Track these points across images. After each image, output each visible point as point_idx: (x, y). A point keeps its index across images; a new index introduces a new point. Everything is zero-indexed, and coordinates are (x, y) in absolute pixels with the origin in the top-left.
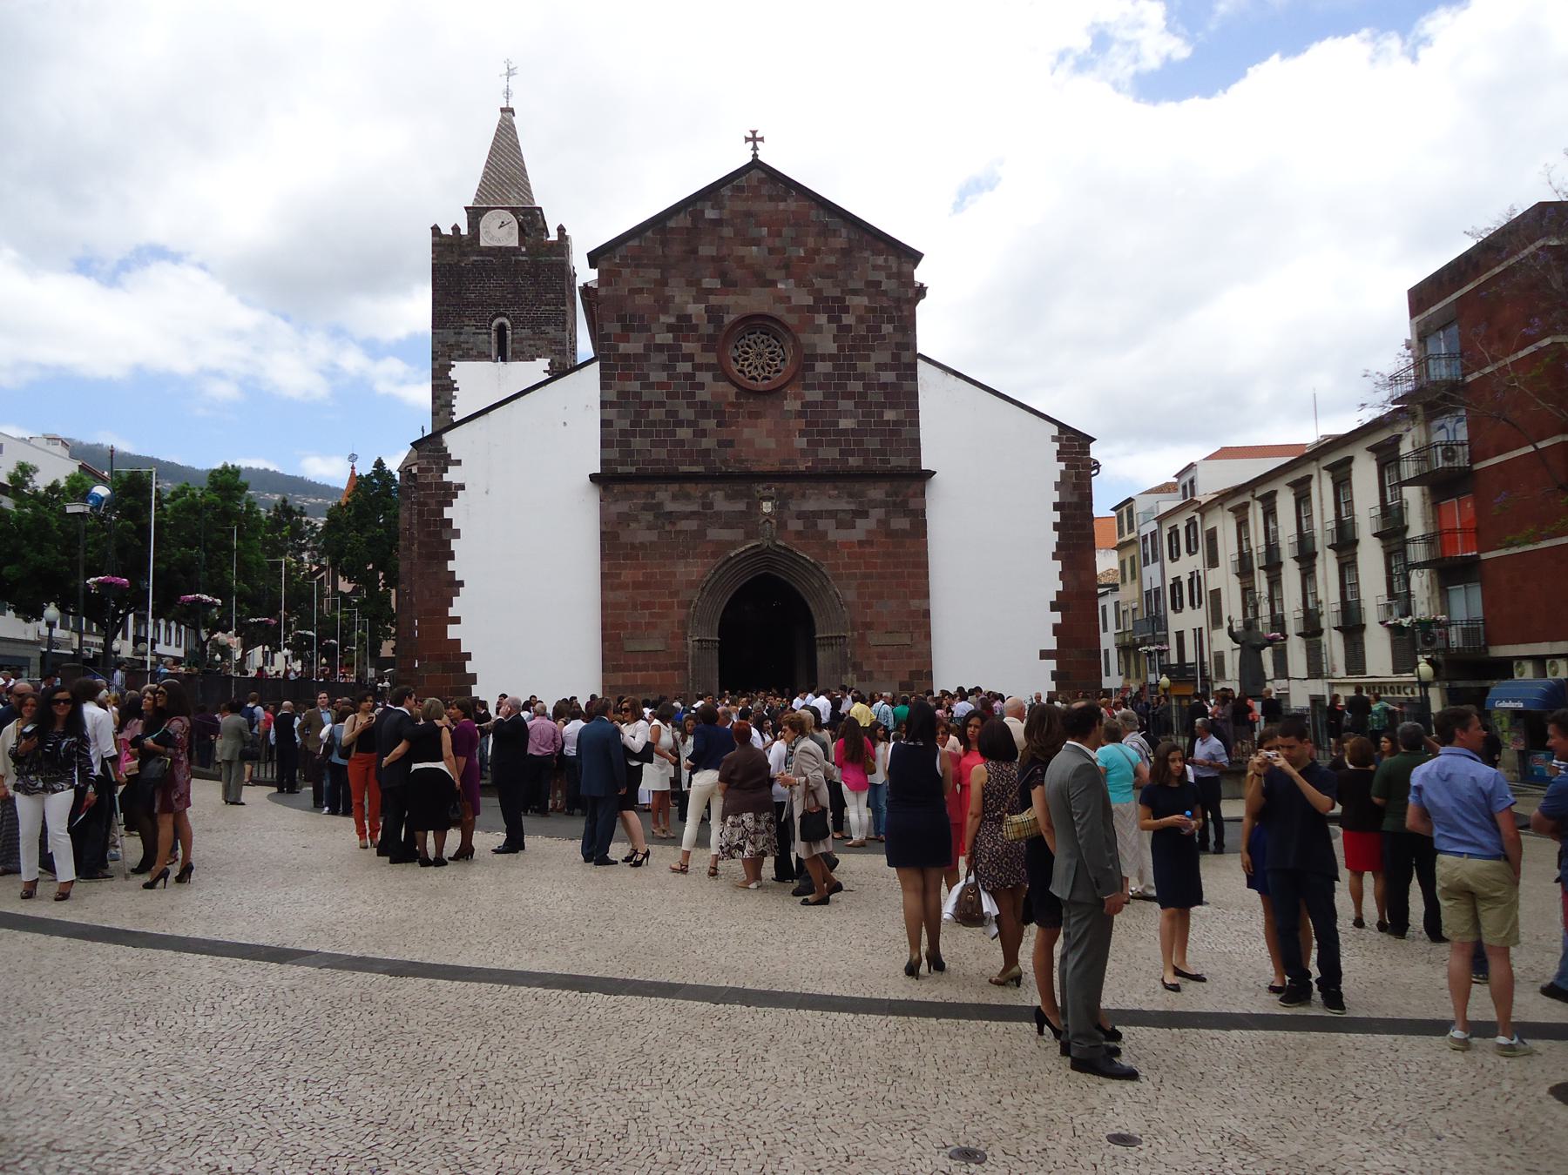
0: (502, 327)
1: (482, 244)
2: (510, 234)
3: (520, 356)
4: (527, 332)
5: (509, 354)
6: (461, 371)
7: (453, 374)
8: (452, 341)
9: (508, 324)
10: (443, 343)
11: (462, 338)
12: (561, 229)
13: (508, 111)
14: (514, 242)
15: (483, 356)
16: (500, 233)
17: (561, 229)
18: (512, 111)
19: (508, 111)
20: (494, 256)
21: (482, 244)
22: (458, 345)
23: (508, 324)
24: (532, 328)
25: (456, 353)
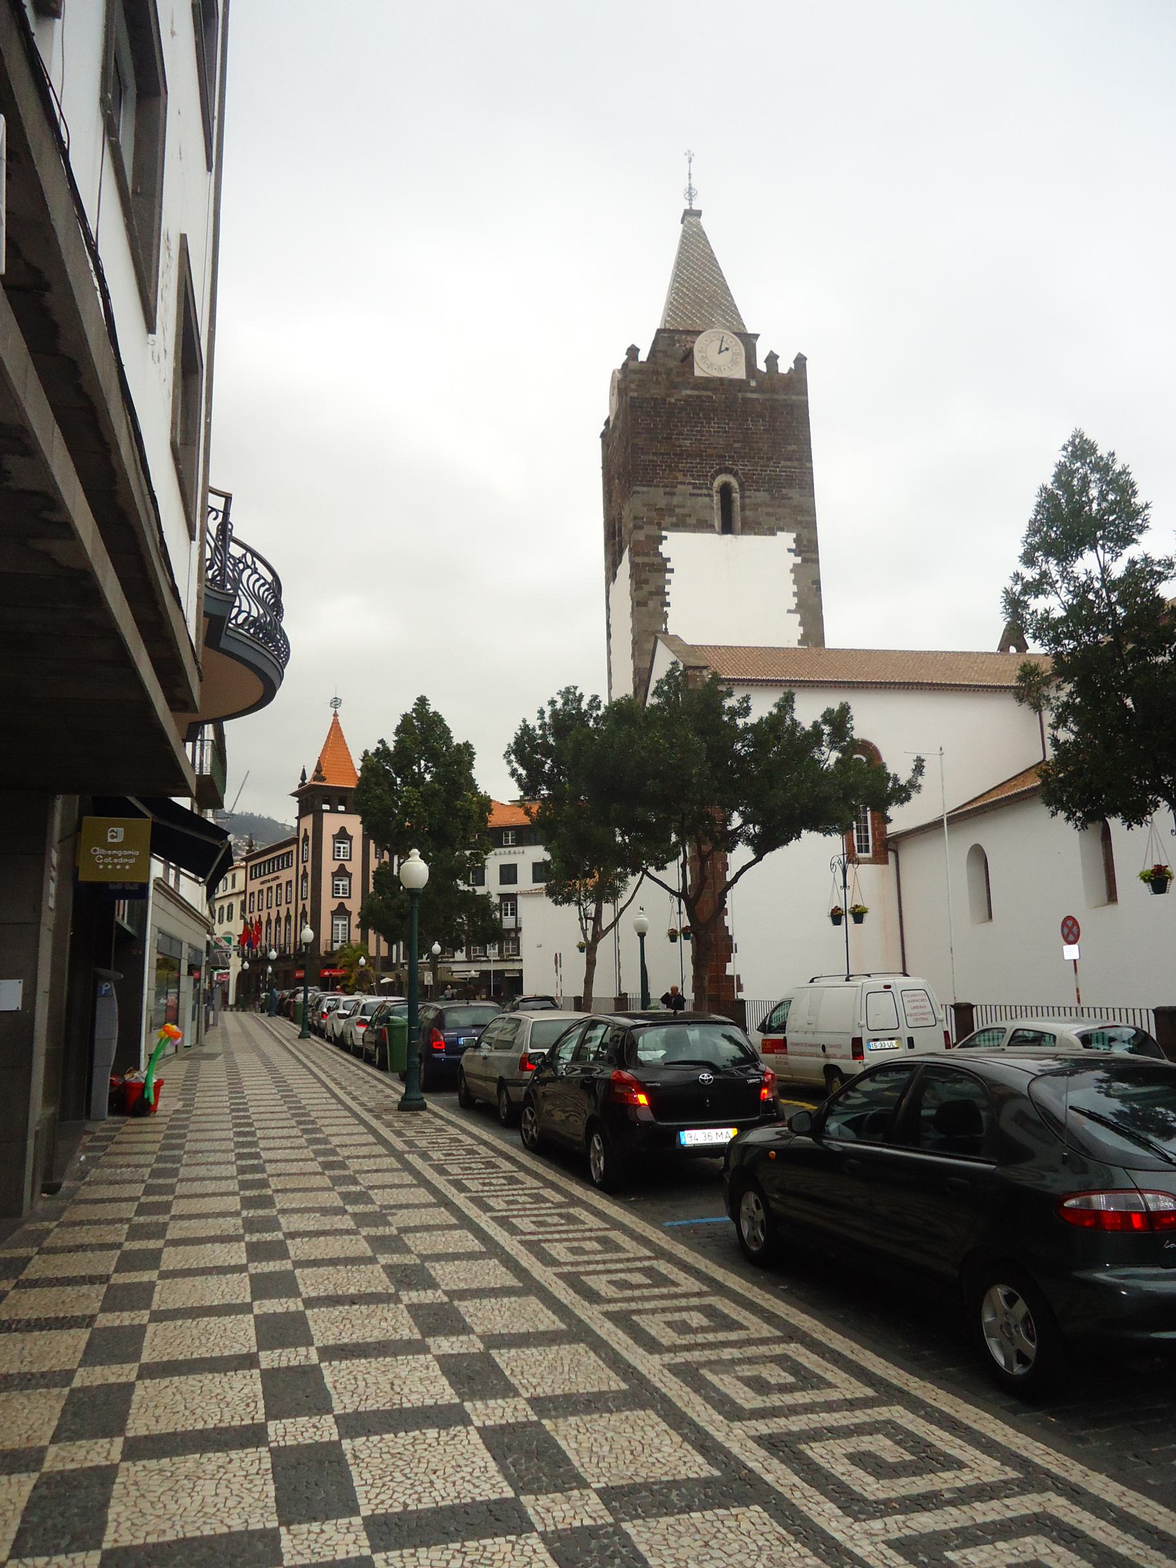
0: (726, 490)
1: (698, 372)
2: (734, 362)
3: (750, 527)
4: (762, 496)
5: (738, 524)
6: (676, 546)
7: (665, 549)
8: (662, 502)
9: (735, 483)
10: (650, 506)
11: (676, 500)
12: (800, 361)
13: (691, 215)
14: (740, 373)
15: (703, 526)
16: (714, 360)
17: (800, 361)
18: (698, 214)
19: (691, 215)
20: (715, 390)
21: (698, 372)
22: (670, 510)
23: (735, 483)
24: (769, 491)
25: (668, 520)
